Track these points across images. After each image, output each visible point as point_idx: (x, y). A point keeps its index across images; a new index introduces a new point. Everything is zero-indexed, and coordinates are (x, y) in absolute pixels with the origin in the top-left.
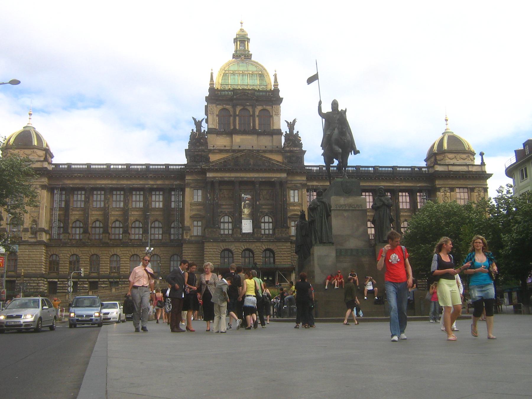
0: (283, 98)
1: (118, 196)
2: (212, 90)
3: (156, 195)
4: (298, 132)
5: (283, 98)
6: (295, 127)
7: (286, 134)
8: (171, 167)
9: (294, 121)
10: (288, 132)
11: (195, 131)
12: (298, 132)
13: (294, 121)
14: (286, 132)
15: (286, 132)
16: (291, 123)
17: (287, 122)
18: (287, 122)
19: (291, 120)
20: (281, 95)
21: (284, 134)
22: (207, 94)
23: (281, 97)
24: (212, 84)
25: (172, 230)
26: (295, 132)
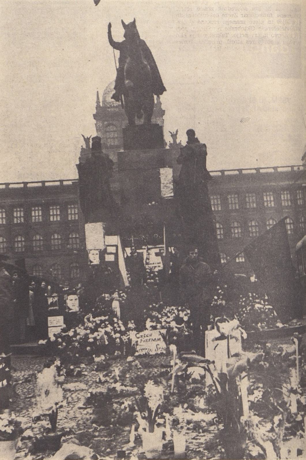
0: (164, 111)
1: (19, 213)
2: (98, 107)
3: (53, 209)
4: (181, 141)
5: (164, 111)
6: (178, 136)
7: (171, 144)
8: (65, 183)
9: (177, 131)
10: (172, 142)
11: (84, 147)
12: (181, 141)
13: (177, 131)
14: (170, 142)
15: (170, 142)
16: (173, 133)
17: (171, 133)
18: (171, 133)
19: (174, 131)
20: (163, 107)
21: (168, 144)
22: (95, 112)
23: (163, 109)
24: (98, 102)
25: (70, 240)
26: (178, 141)
